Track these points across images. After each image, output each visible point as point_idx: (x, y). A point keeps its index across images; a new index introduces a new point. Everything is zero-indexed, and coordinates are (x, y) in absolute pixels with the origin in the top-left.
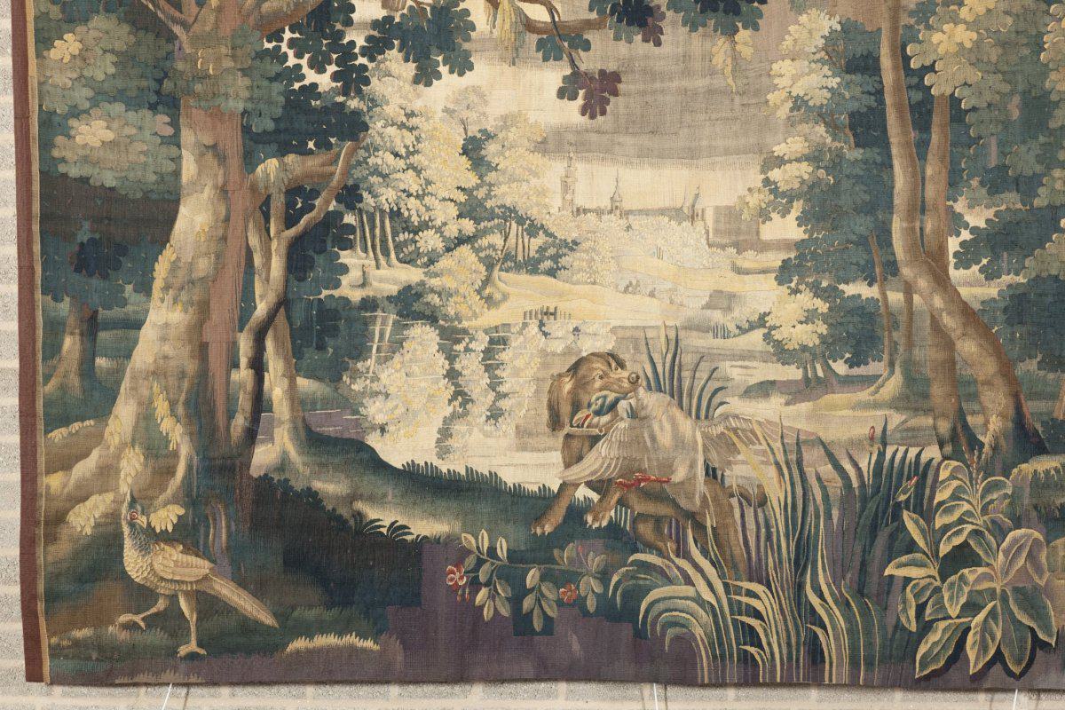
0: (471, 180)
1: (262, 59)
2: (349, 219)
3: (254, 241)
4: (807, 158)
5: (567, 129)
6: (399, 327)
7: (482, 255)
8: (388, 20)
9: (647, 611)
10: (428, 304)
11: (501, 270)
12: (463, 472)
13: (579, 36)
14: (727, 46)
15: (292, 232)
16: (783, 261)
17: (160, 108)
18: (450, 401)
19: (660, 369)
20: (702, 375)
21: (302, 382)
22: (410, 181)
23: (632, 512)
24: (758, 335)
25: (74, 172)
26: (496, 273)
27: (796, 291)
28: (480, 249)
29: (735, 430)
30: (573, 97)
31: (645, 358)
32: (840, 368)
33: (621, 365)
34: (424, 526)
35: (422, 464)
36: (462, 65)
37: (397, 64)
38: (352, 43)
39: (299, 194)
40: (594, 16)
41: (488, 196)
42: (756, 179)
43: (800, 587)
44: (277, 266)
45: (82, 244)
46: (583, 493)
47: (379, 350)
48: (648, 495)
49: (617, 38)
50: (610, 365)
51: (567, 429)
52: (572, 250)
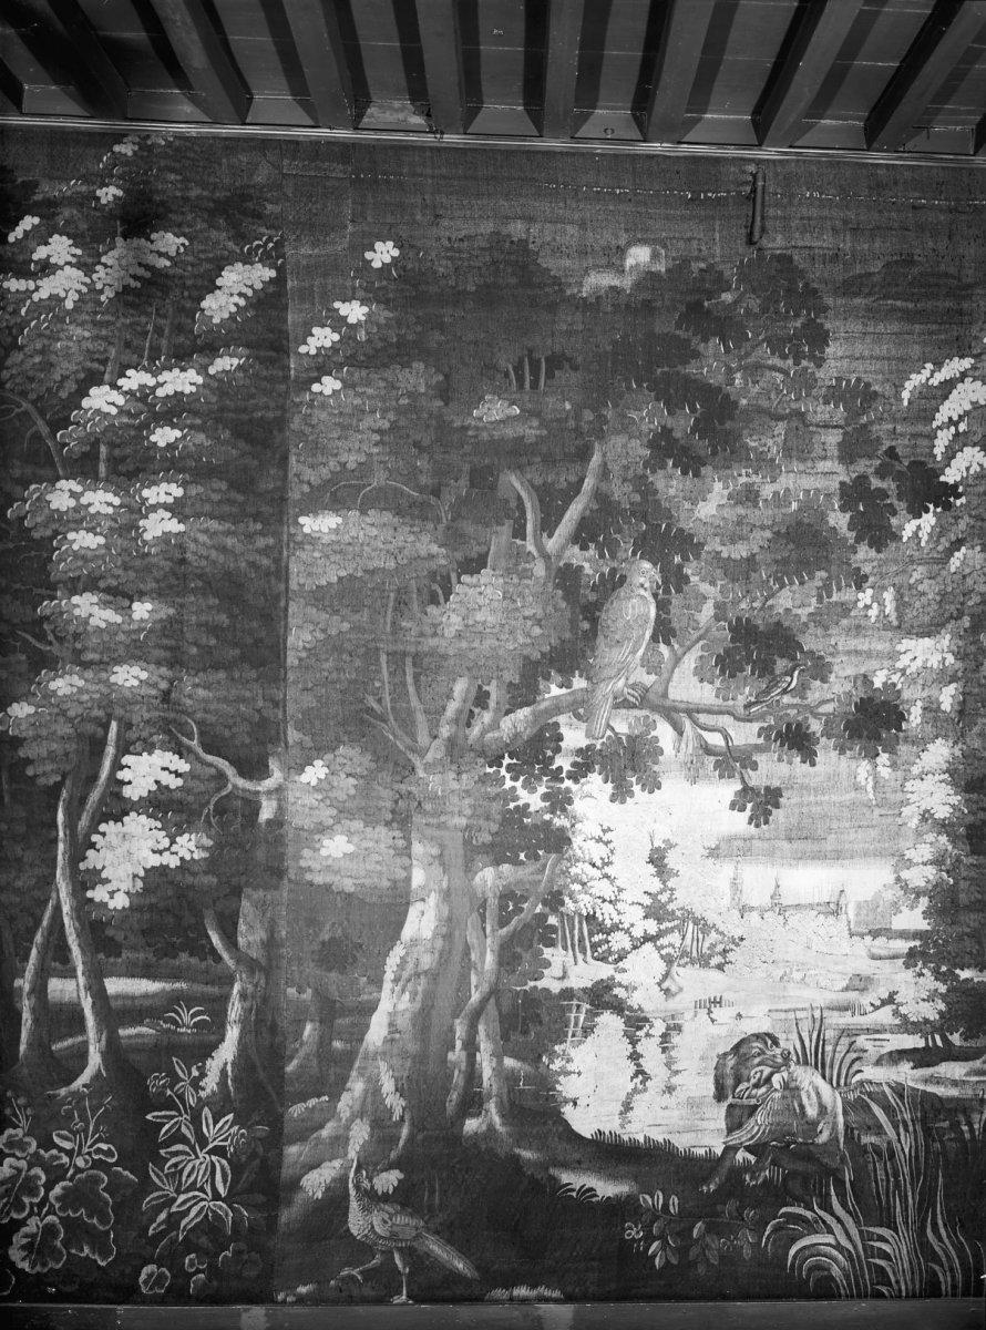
0: (655, 885)
1: (484, 782)
2: (552, 920)
3: (472, 938)
4: (932, 863)
5: (735, 838)
6: (592, 1015)
7: (663, 952)
8: (589, 748)
9: (795, 1257)
10: (616, 996)
11: (679, 965)
12: (642, 1140)
13: (750, 757)
14: (869, 767)
15: (504, 931)
16: (911, 949)
17: (395, 825)
18: (632, 1078)
21: (509, 1062)
22: (604, 888)
25: (319, 879)
26: (675, 968)
27: (921, 975)
28: (662, 947)
29: (870, 1095)
30: (742, 809)
31: (795, 1036)
32: (956, 1039)
33: (776, 1042)
34: (606, 1189)
35: (607, 1133)
36: (653, 785)
37: (595, 782)
38: (560, 769)
39: (510, 897)
40: (761, 741)
41: (670, 900)
42: (891, 879)
43: (922, 1229)
44: (490, 960)
45: (323, 943)
46: (741, 1155)
47: (573, 1036)
48: (796, 1156)
49: (780, 760)
50: (766, 1043)
51: (730, 1100)
52: (737, 945)
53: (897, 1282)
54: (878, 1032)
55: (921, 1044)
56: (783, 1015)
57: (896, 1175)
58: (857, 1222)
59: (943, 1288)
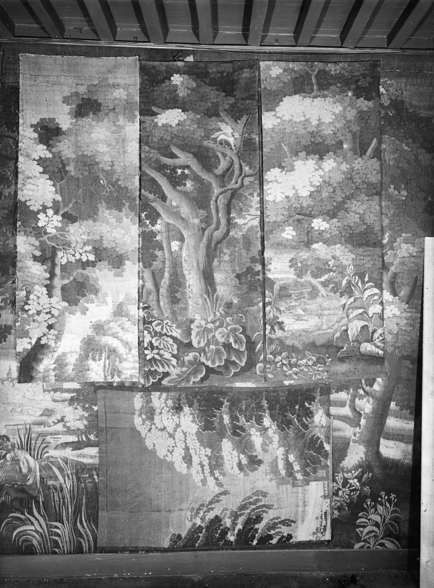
9: (16, 536)
16: (71, 397)
19: (23, 440)
20: (39, 442)
23: (11, 497)
24: (61, 424)
27: (76, 408)
29: (52, 463)
32: (92, 437)
43: (75, 523)
53: (63, 547)
54: (56, 434)
55: (76, 439)
56: (12, 427)
57: (63, 498)
58: (45, 520)
59: (84, 549)
